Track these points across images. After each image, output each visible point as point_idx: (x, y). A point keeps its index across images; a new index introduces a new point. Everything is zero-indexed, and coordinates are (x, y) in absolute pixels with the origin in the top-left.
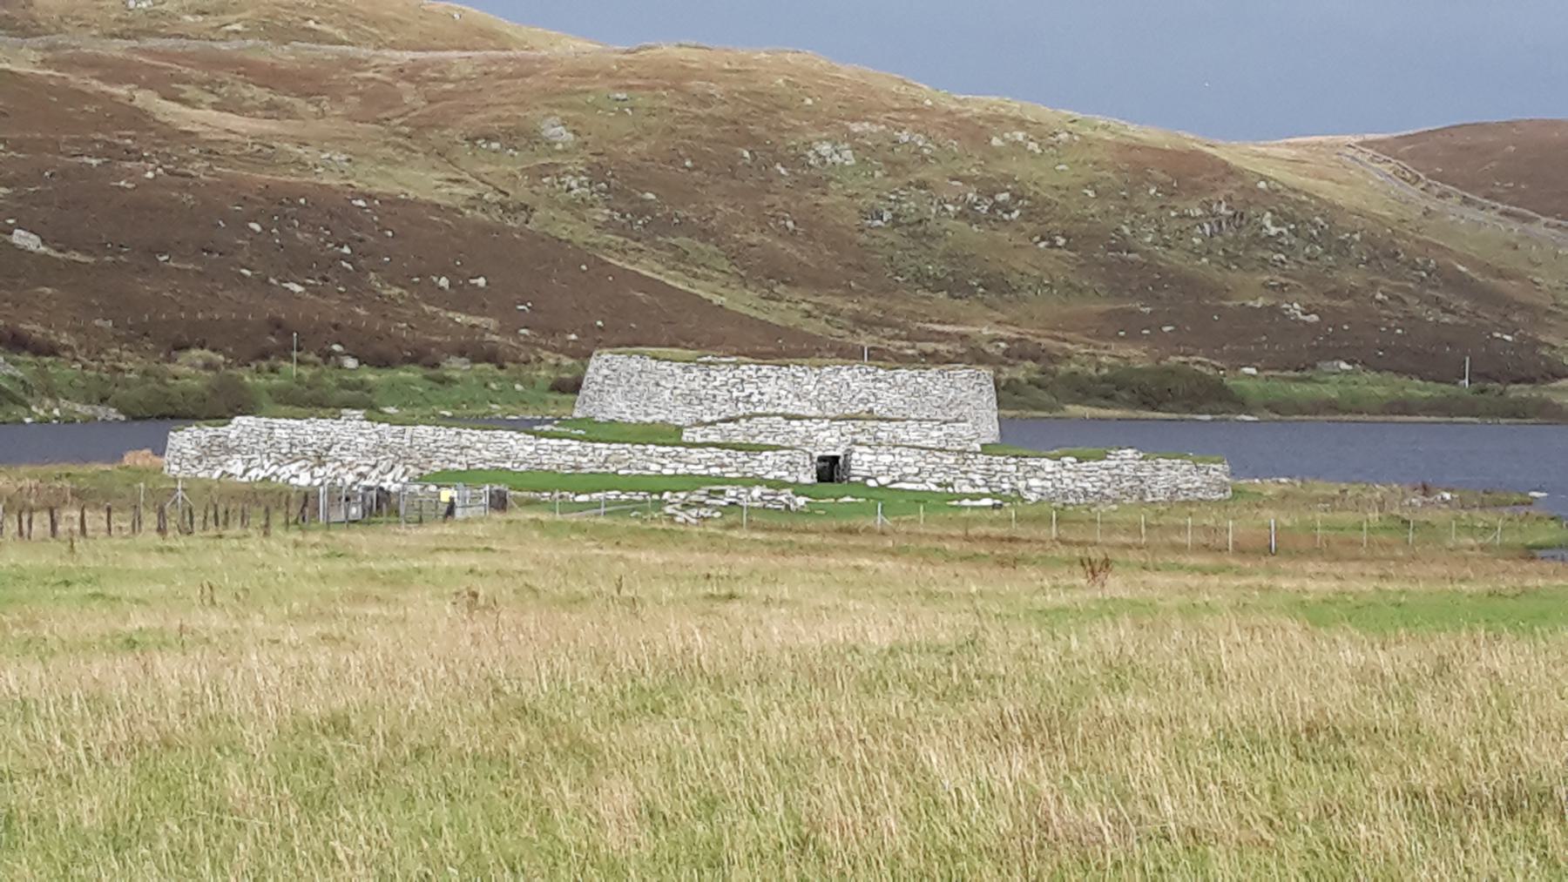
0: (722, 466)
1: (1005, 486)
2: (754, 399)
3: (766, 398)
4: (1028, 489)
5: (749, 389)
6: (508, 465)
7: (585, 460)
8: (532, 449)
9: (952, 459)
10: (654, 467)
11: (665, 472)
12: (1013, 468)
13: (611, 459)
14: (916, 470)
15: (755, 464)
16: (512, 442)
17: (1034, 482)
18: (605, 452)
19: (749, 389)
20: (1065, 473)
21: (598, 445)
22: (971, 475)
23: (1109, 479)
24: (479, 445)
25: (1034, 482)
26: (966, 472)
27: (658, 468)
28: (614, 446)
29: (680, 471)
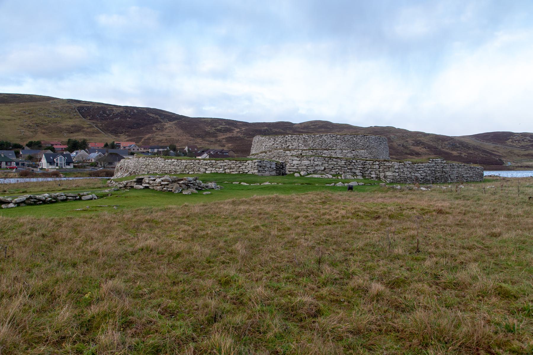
0: (231, 168)
1: (373, 176)
2: (290, 147)
3: (294, 147)
4: (385, 177)
7: (178, 168)
9: (343, 162)
10: (202, 170)
11: (207, 172)
12: (377, 166)
13: (187, 167)
14: (323, 168)
15: (243, 167)
17: (388, 174)
20: (405, 169)
21: (183, 161)
22: (353, 170)
23: (429, 172)
25: (388, 174)
26: (351, 169)
27: (204, 171)
28: (188, 161)
29: (213, 172)
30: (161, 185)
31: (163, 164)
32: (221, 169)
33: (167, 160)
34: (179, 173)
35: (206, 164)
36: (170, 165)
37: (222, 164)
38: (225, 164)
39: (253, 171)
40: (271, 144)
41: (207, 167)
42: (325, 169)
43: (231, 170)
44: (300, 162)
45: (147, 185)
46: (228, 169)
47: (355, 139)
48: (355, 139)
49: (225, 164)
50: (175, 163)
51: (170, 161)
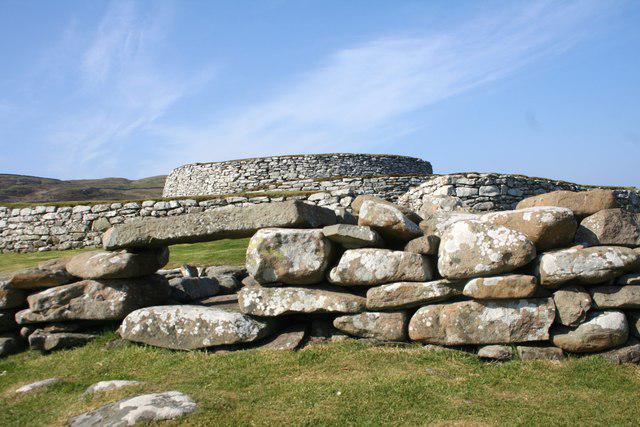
5: (273, 175)
7: (62, 230)
13: (97, 225)
18: (85, 218)
21: (78, 209)
28: (97, 208)
33: (15, 211)
34: (66, 245)
44: (475, 190)
47: (401, 165)
48: (401, 165)
50: (46, 217)
51: (26, 211)
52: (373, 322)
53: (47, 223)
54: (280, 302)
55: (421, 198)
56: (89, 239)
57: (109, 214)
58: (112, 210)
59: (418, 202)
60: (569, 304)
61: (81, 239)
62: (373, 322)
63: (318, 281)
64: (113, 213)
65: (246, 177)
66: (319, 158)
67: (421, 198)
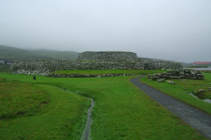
2: (110, 57)
6: (73, 68)
7: (93, 66)
8: (79, 64)
16: (74, 63)
19: (109, 56)
24: (66, 64)
30: (197, 76)
31: (79, 64)
32: (122, 67)
35: (112, 65)
36: (86, 65)
37: (121, 64)
38: (123, 64)
39: (141, 68)
40: (100, 55)
41: (113, 66)
42: (168, 67)
43: (127, 68)
45: (184, 76)
46: (125, 67)
49: (123, 64)
50: (89, 64)
52: (187, 78)
53: (90, 65)
54: (182, 76)
55: (151, 64)
56: (98, 68)
57: (102, 64)
58: (102, 63)
59: (150, 64)
60: (198, 77)
61: (96, 68)
62: (187, 78)
63: (184, 75)
64: (103, 64)
65: (103, 56)
66: (118, 52)
67: (151, 64)
